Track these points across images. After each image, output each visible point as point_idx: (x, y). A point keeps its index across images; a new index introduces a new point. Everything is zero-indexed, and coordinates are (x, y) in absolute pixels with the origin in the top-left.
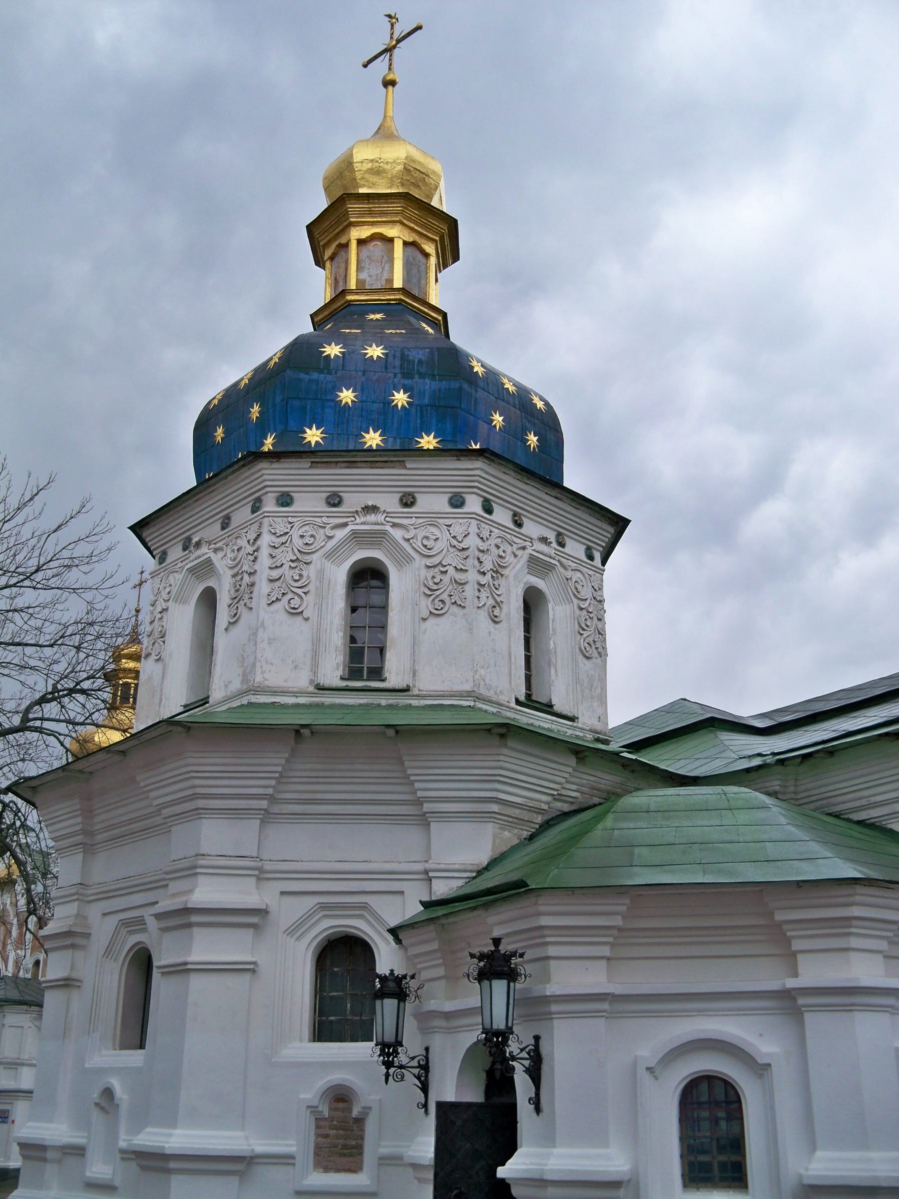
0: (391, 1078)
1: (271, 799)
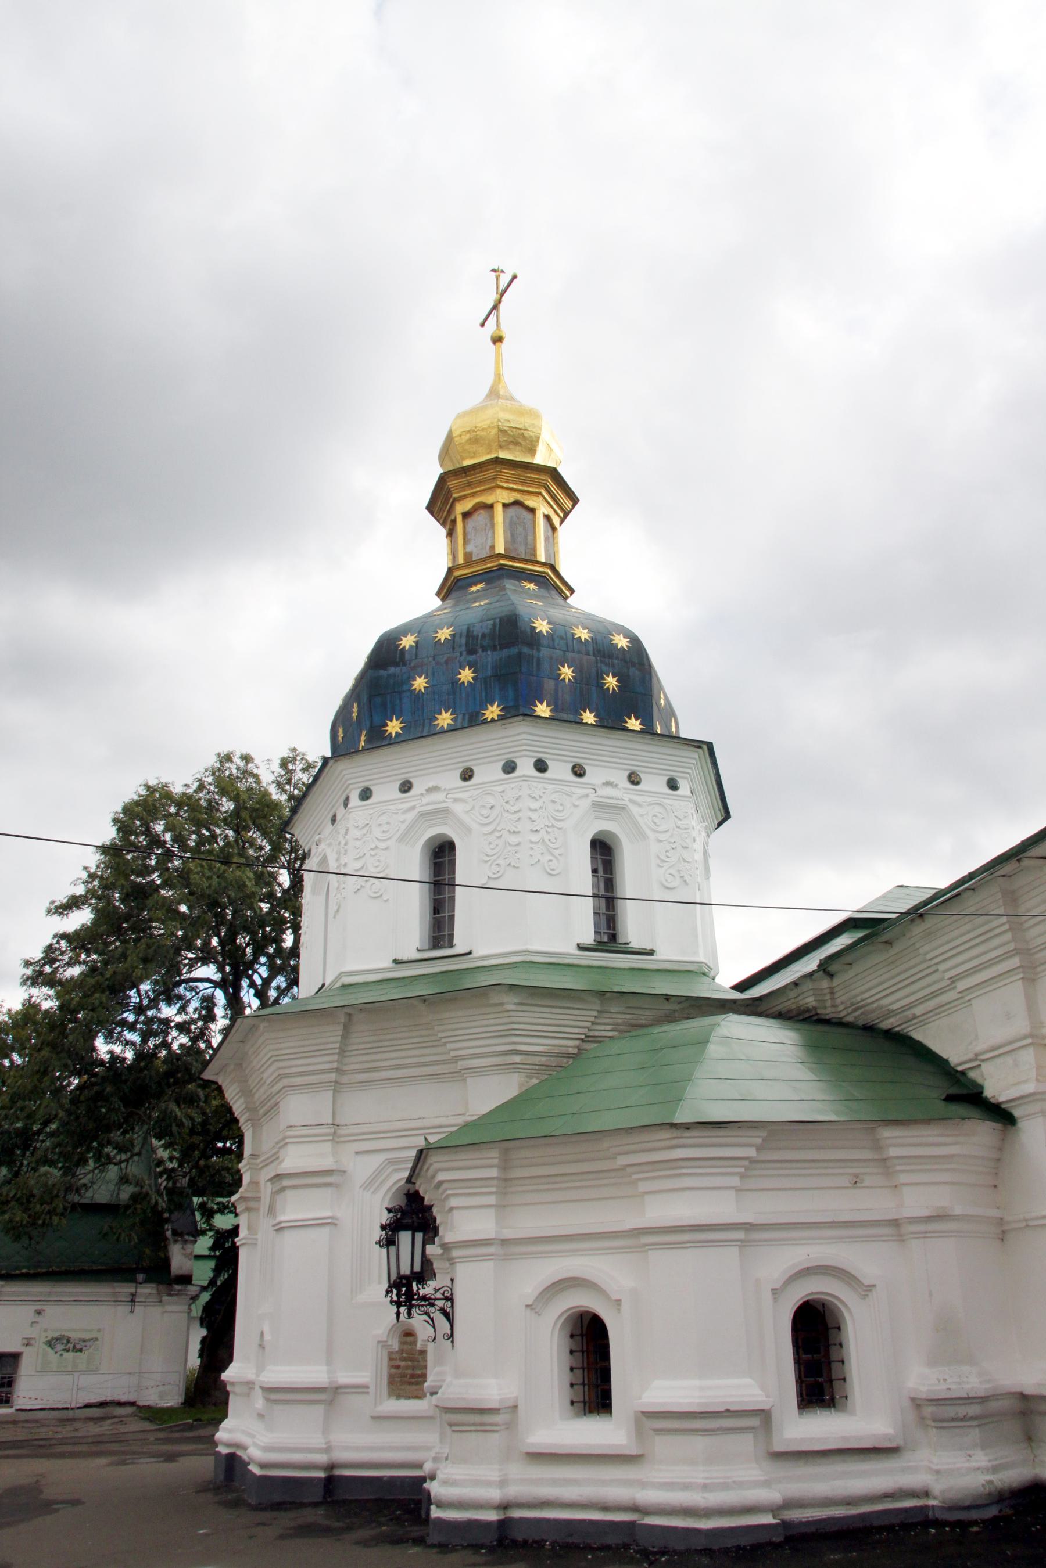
0: (401, 1316)
1: (338, 1070)
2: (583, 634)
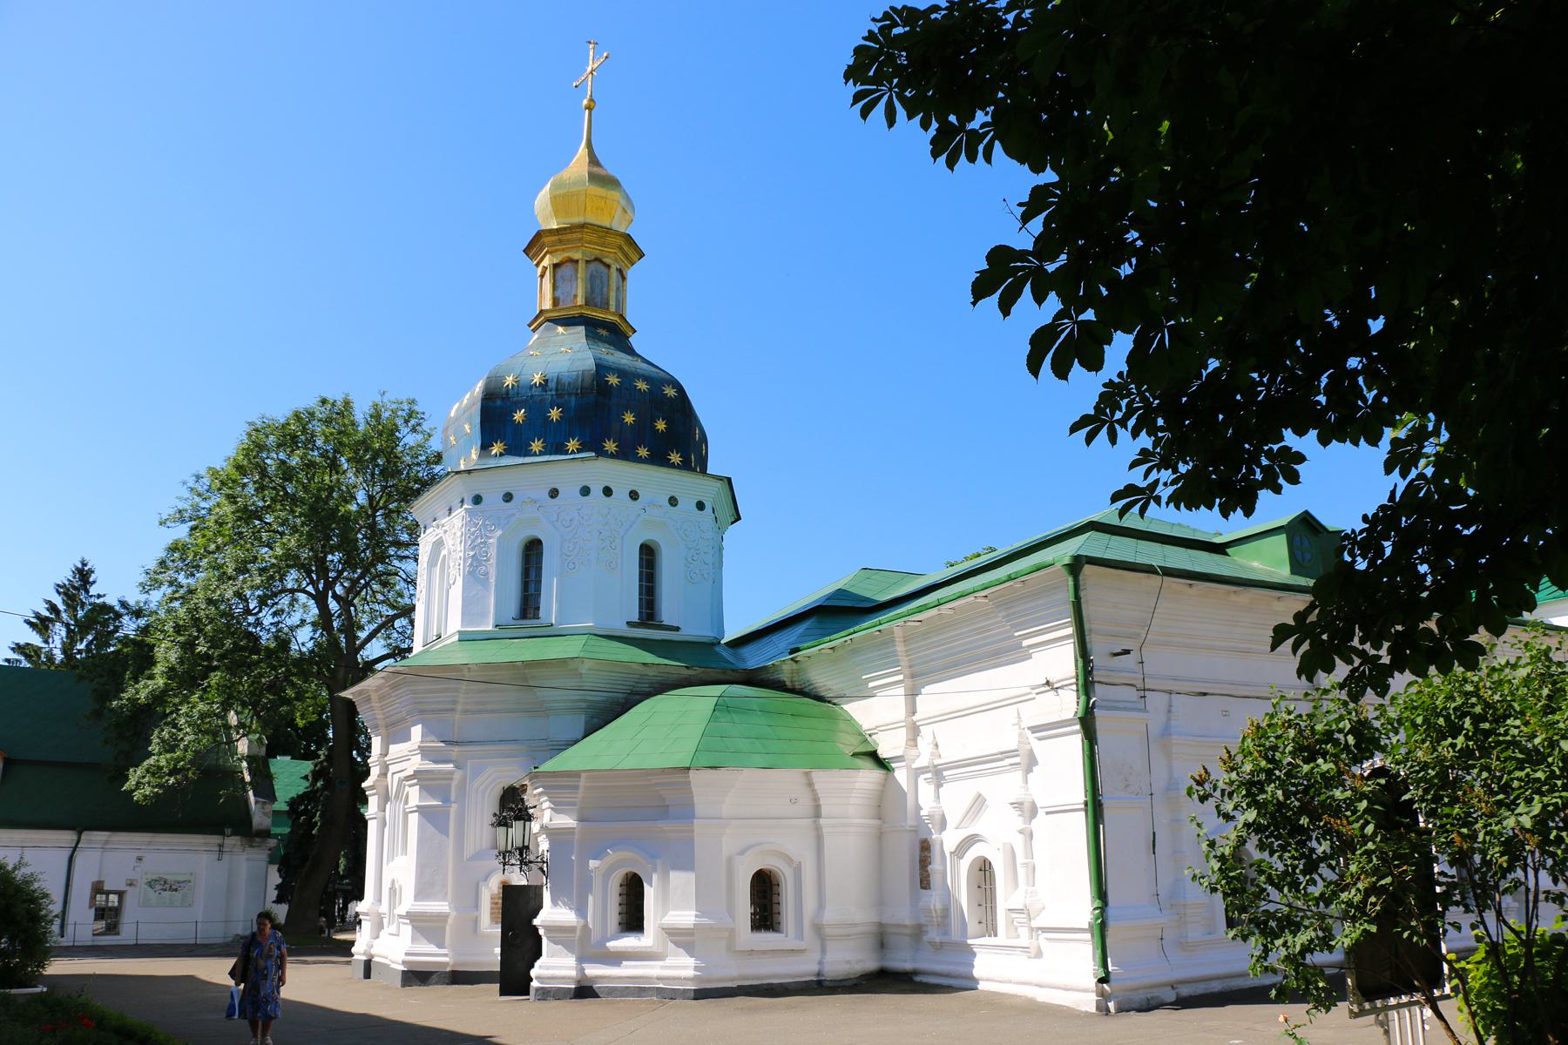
2: (642, 386)
